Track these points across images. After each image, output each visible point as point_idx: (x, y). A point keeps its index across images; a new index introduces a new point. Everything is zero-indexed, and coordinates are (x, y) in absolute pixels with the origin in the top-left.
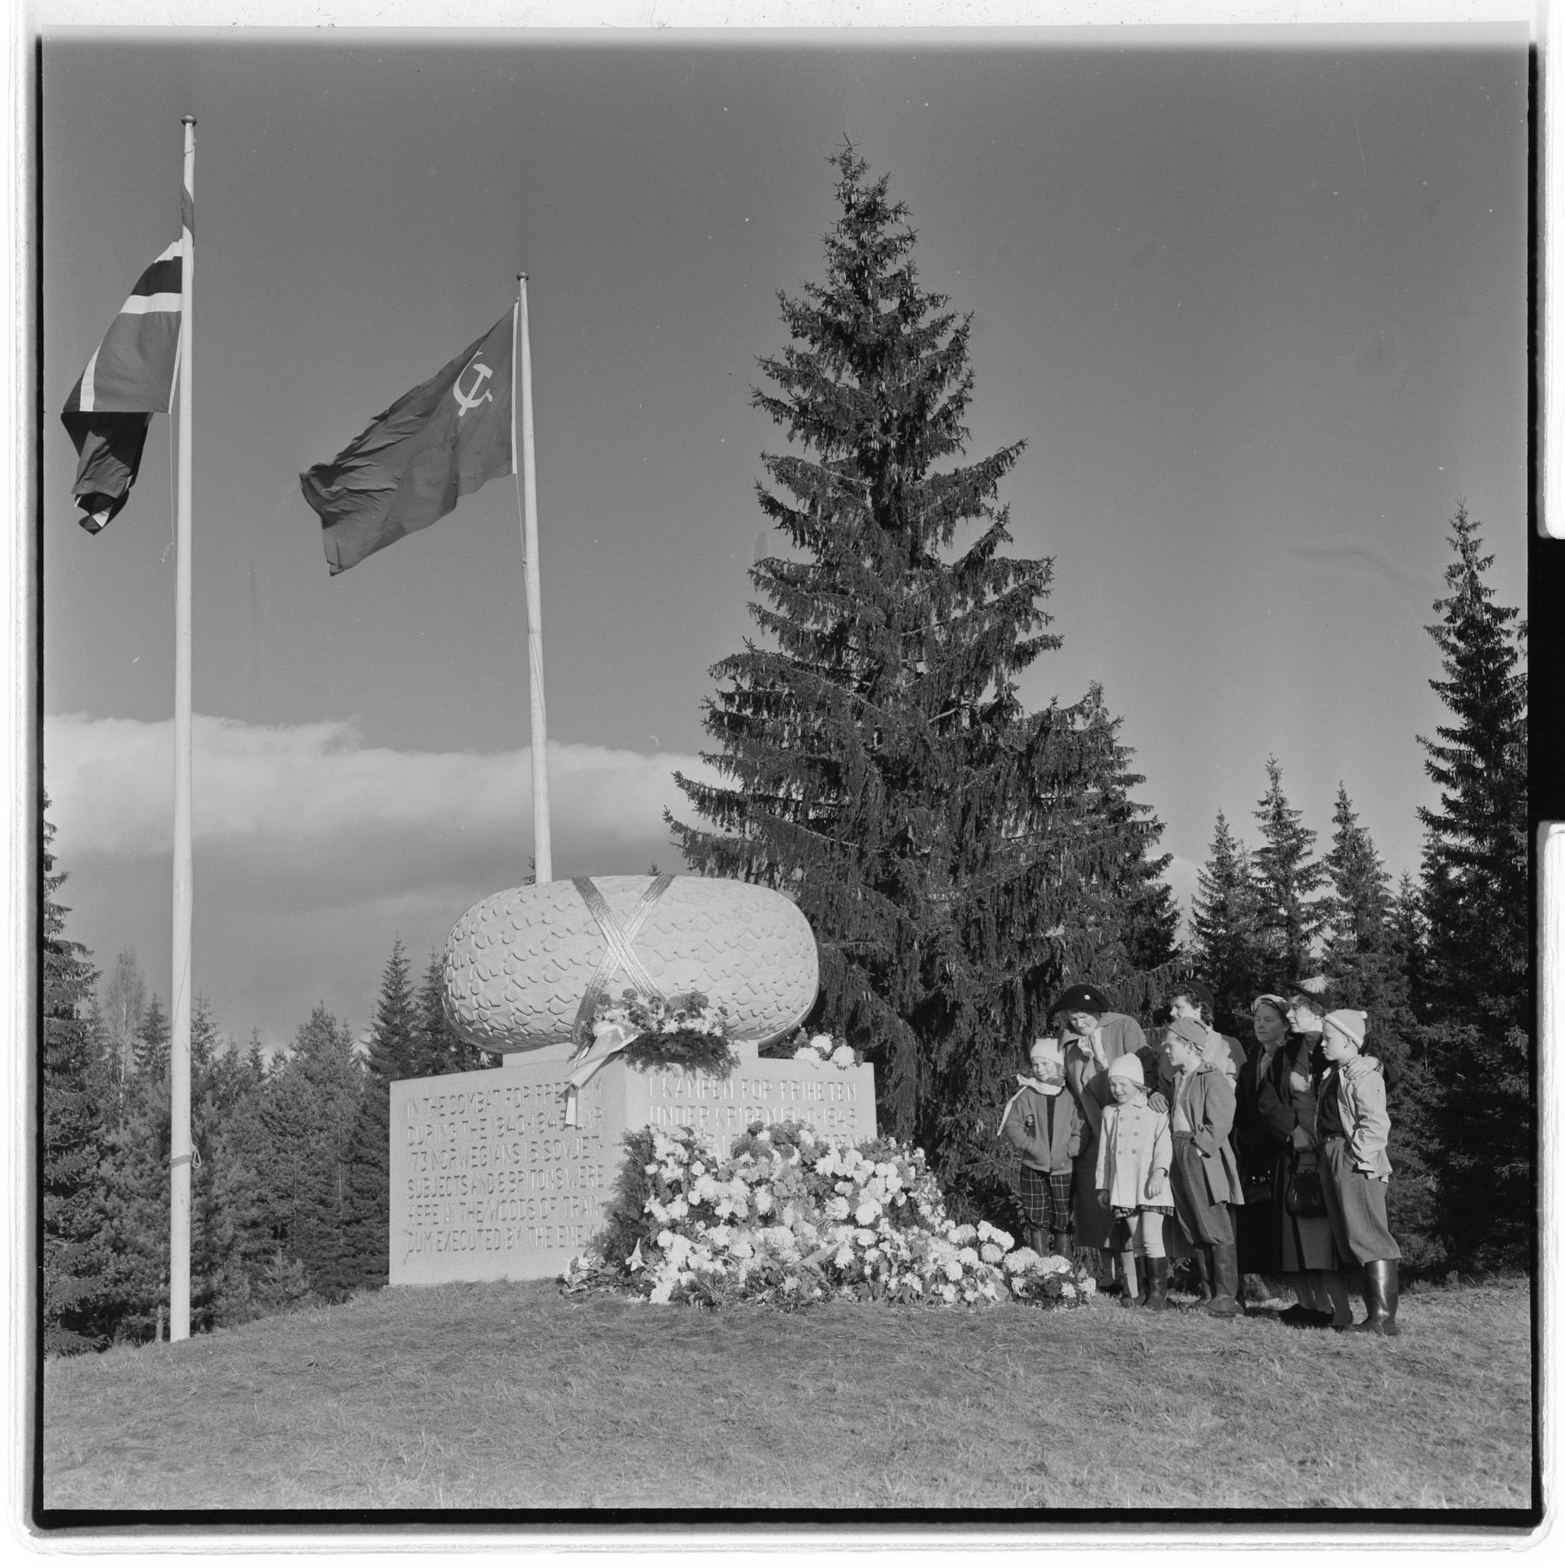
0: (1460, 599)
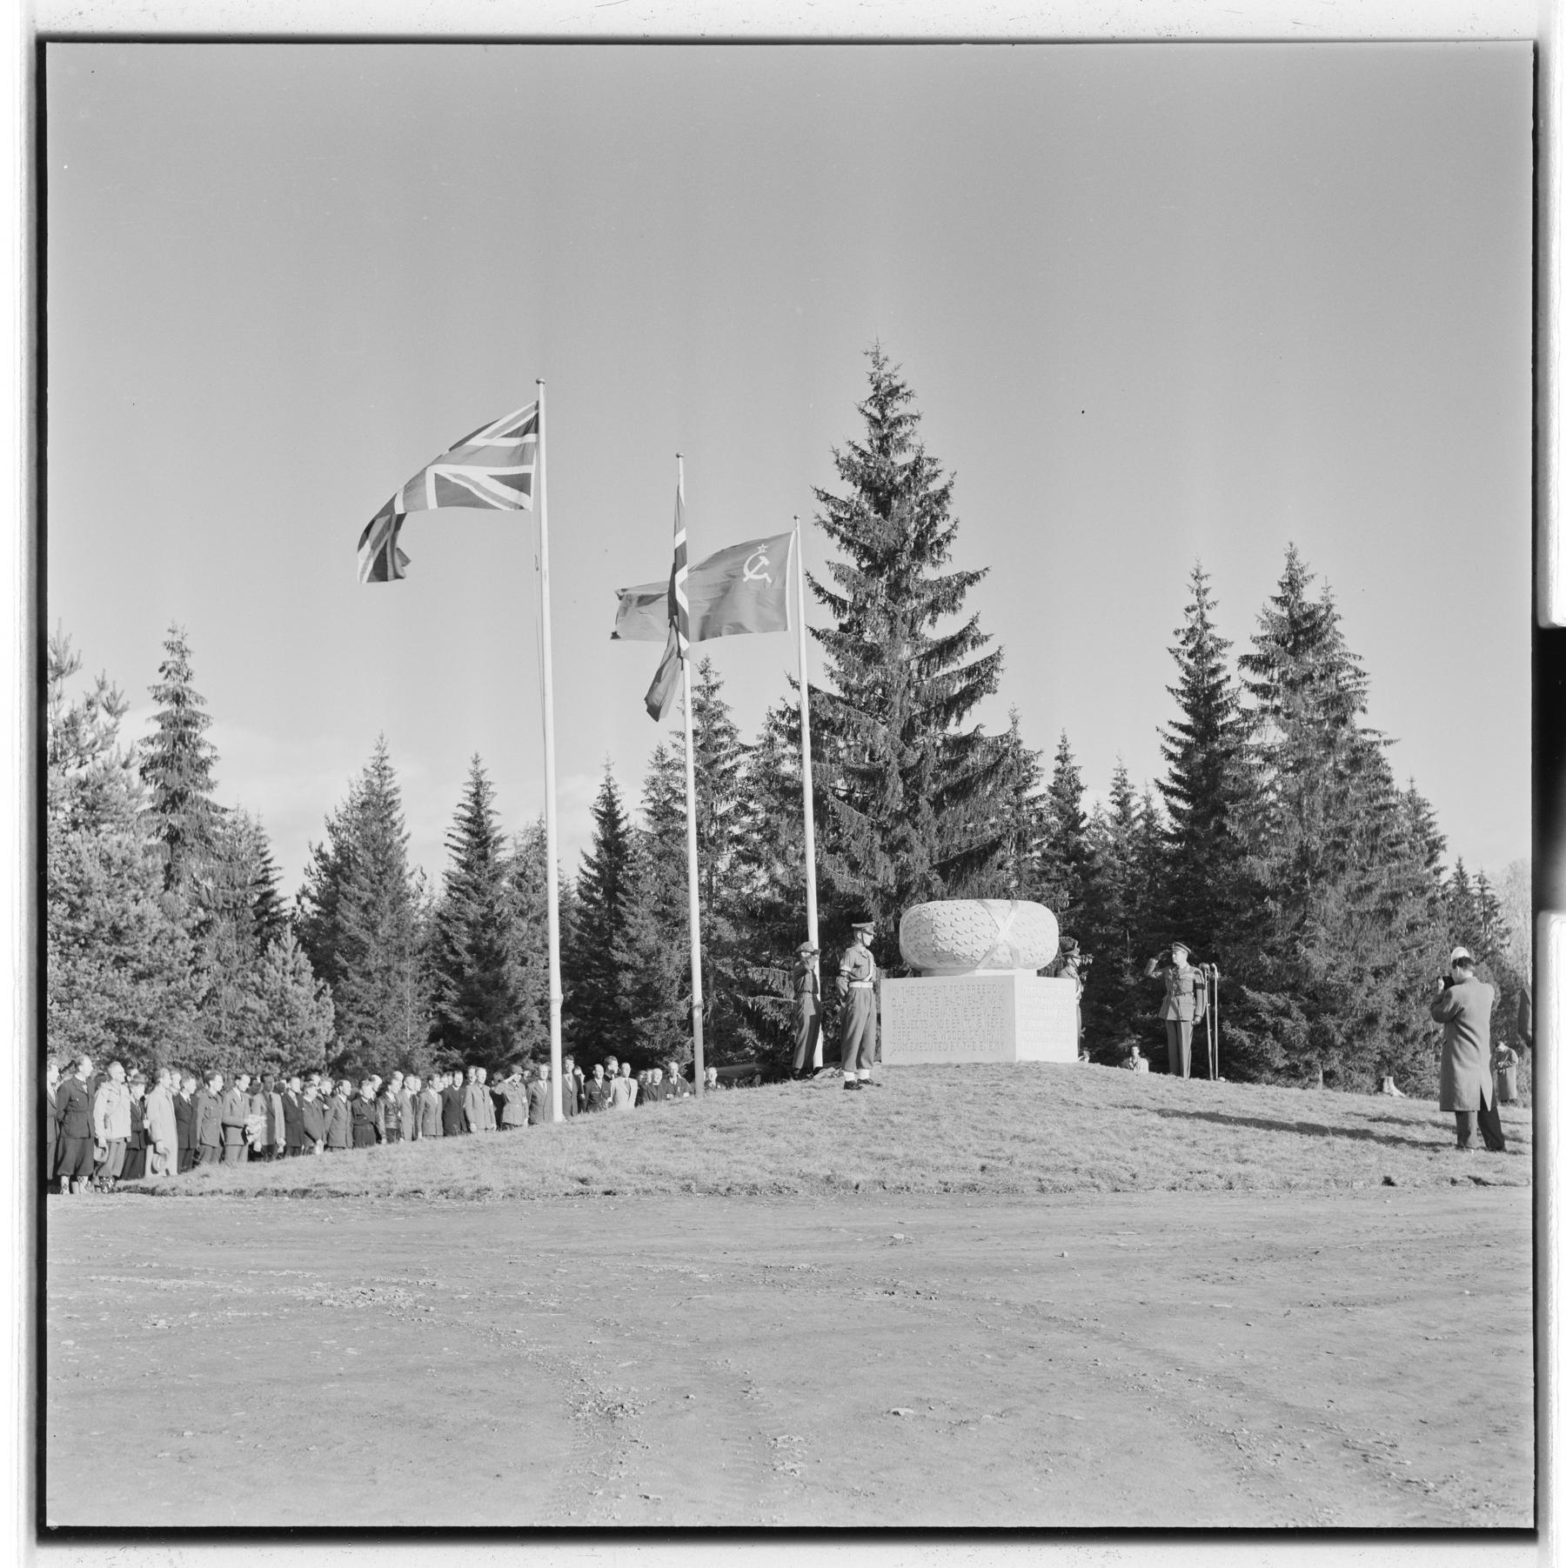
0: (1192, 630)
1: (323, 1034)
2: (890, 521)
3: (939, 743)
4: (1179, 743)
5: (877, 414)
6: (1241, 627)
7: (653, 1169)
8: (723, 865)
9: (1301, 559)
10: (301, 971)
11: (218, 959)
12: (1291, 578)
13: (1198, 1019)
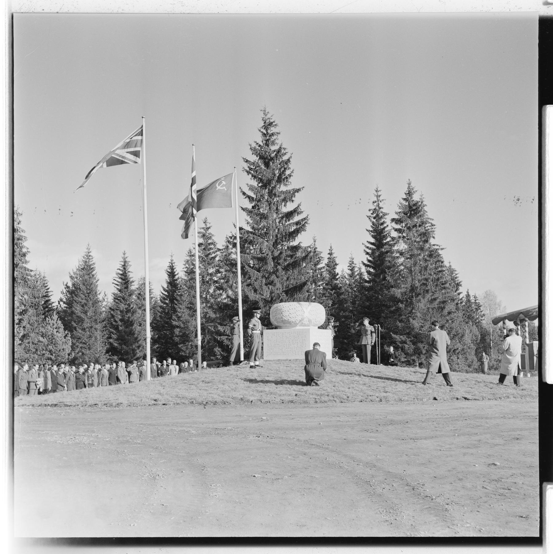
0: (375, 209)
1: (67, 350)
2: (269, 169)
3: (286, 248)
4: (370, 249)
5: (265, 132)
6: (392, 209)
7: (180, 396)
8: (211, 291)
9: (413, 185)
10: (59, 328)
11: (29, 323)
12: (409, 191)
13: (373, 344)
